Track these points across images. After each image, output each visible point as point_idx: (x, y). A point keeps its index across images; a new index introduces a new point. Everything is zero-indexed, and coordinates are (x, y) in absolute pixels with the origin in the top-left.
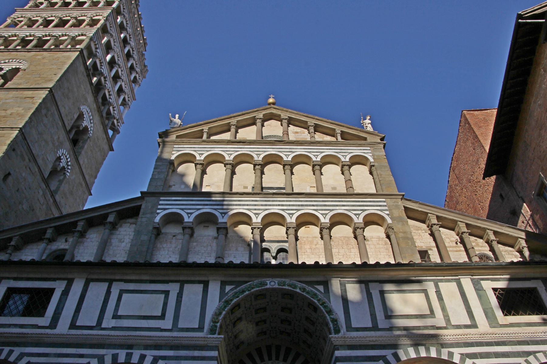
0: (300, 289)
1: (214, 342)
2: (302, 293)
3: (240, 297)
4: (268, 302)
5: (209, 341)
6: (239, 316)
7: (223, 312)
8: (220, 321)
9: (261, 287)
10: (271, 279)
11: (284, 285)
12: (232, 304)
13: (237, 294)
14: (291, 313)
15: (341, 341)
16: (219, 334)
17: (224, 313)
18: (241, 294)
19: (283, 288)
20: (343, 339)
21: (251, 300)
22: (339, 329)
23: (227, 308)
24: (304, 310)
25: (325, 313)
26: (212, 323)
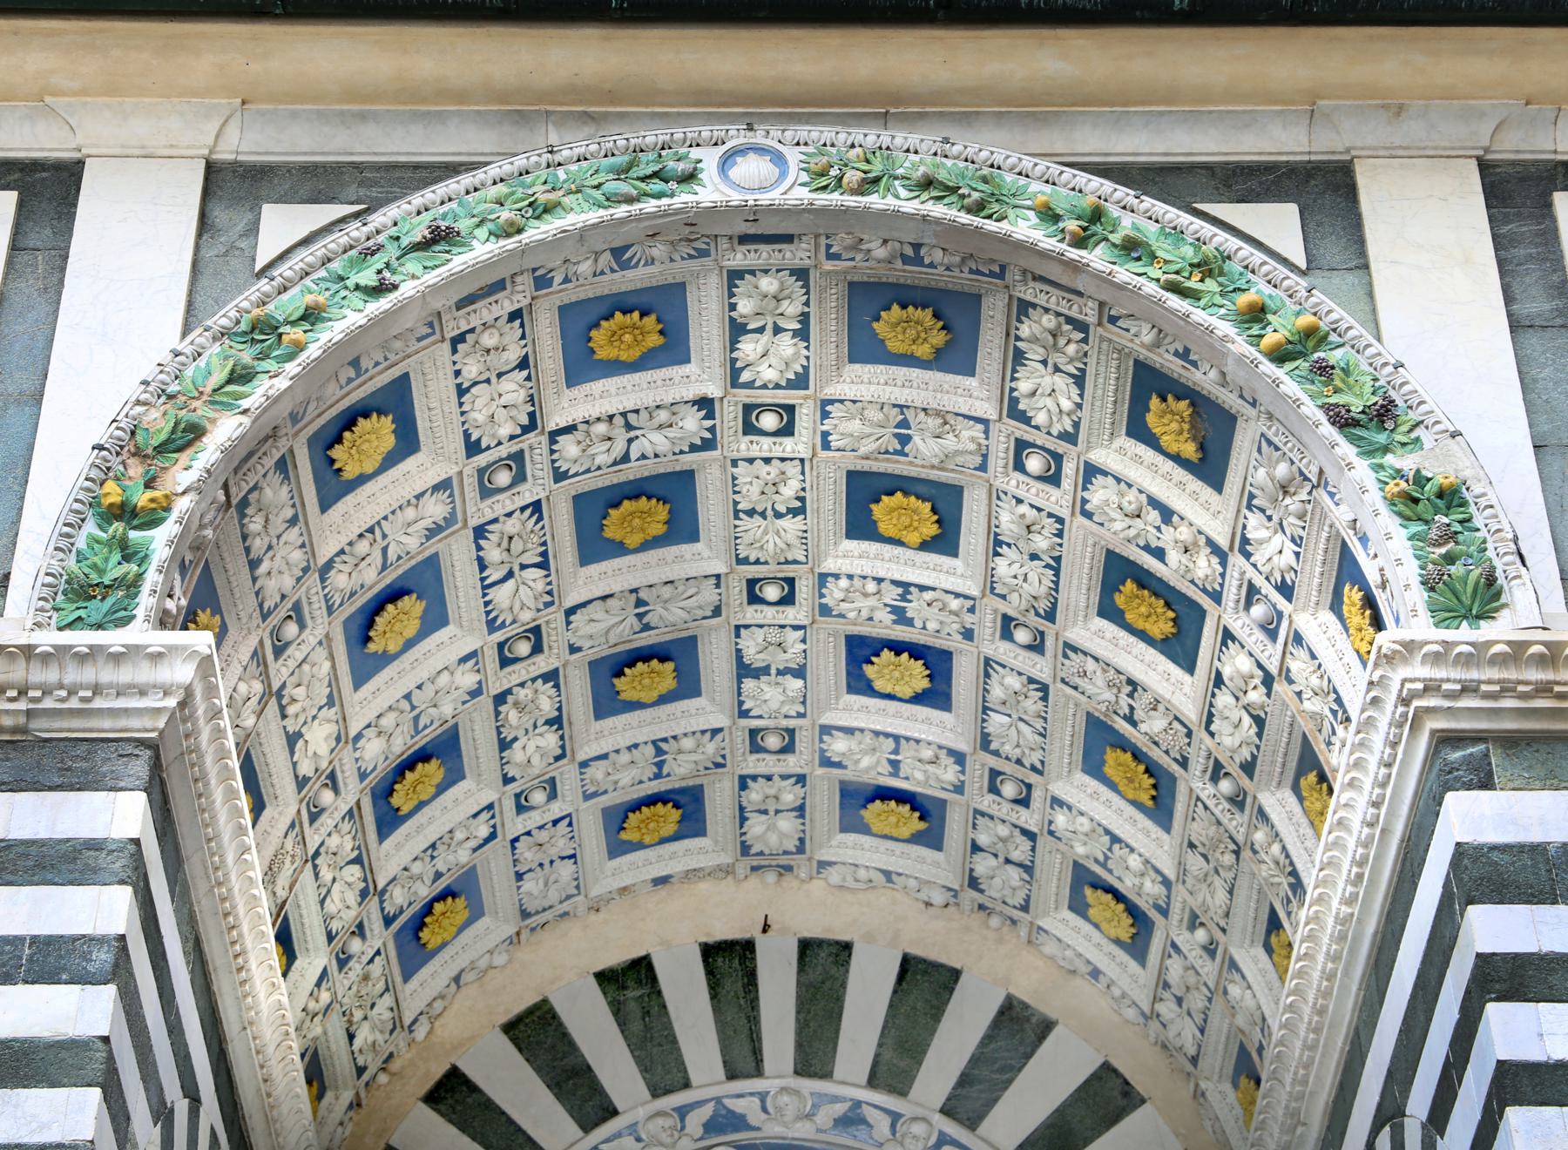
0: (1049, 215)
1: (98, 703)
2: (1074, 254)
3: (407, 289)
4: (705, 404)
5: (47, 691)
6: (408, 543)
7: (213, 421)
8: (183, 504)
9: (630, 200)
10: (737, 137)
11: (870, 184)
12: (313, 351)
13: (378, 261)
14: (944, 541)
15: (1507, 689)
16: (164, 621)
17: (225, 430)
18: (412, 265)
19: (867, 212)
20: (1536, 675)
21: (523, 364)
22: (1491, 580)
23: (260, 391)
24: (1091, 472)
25: (1328, 430)
26: (90, 527)
